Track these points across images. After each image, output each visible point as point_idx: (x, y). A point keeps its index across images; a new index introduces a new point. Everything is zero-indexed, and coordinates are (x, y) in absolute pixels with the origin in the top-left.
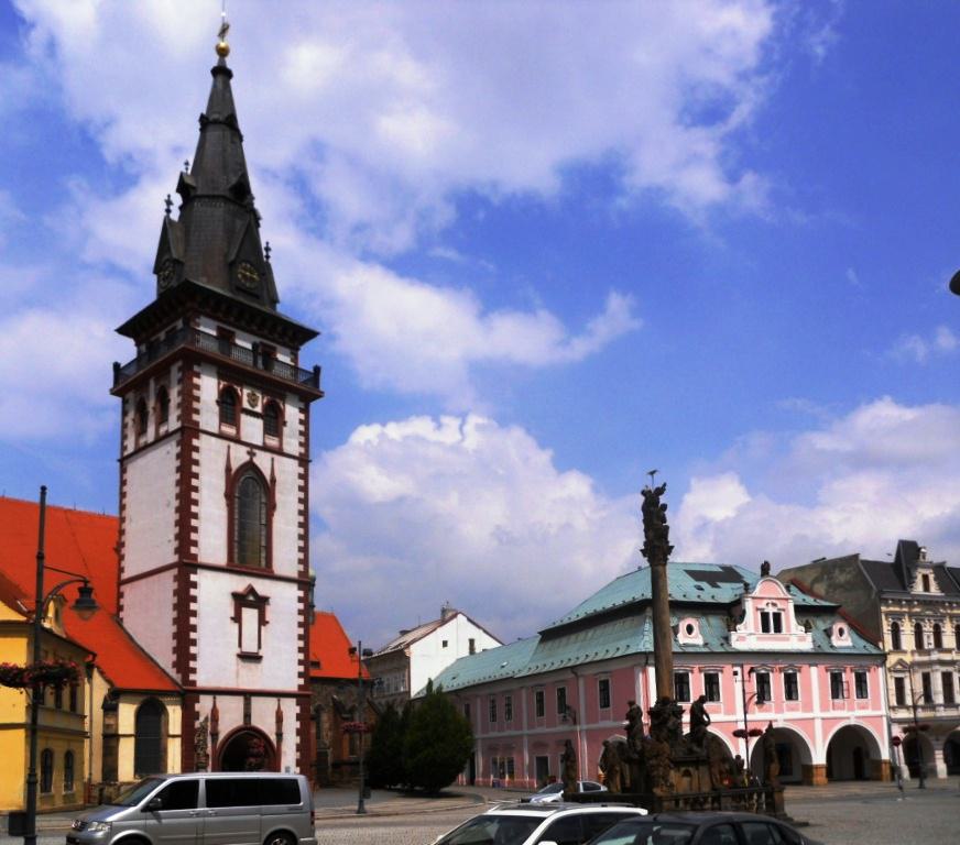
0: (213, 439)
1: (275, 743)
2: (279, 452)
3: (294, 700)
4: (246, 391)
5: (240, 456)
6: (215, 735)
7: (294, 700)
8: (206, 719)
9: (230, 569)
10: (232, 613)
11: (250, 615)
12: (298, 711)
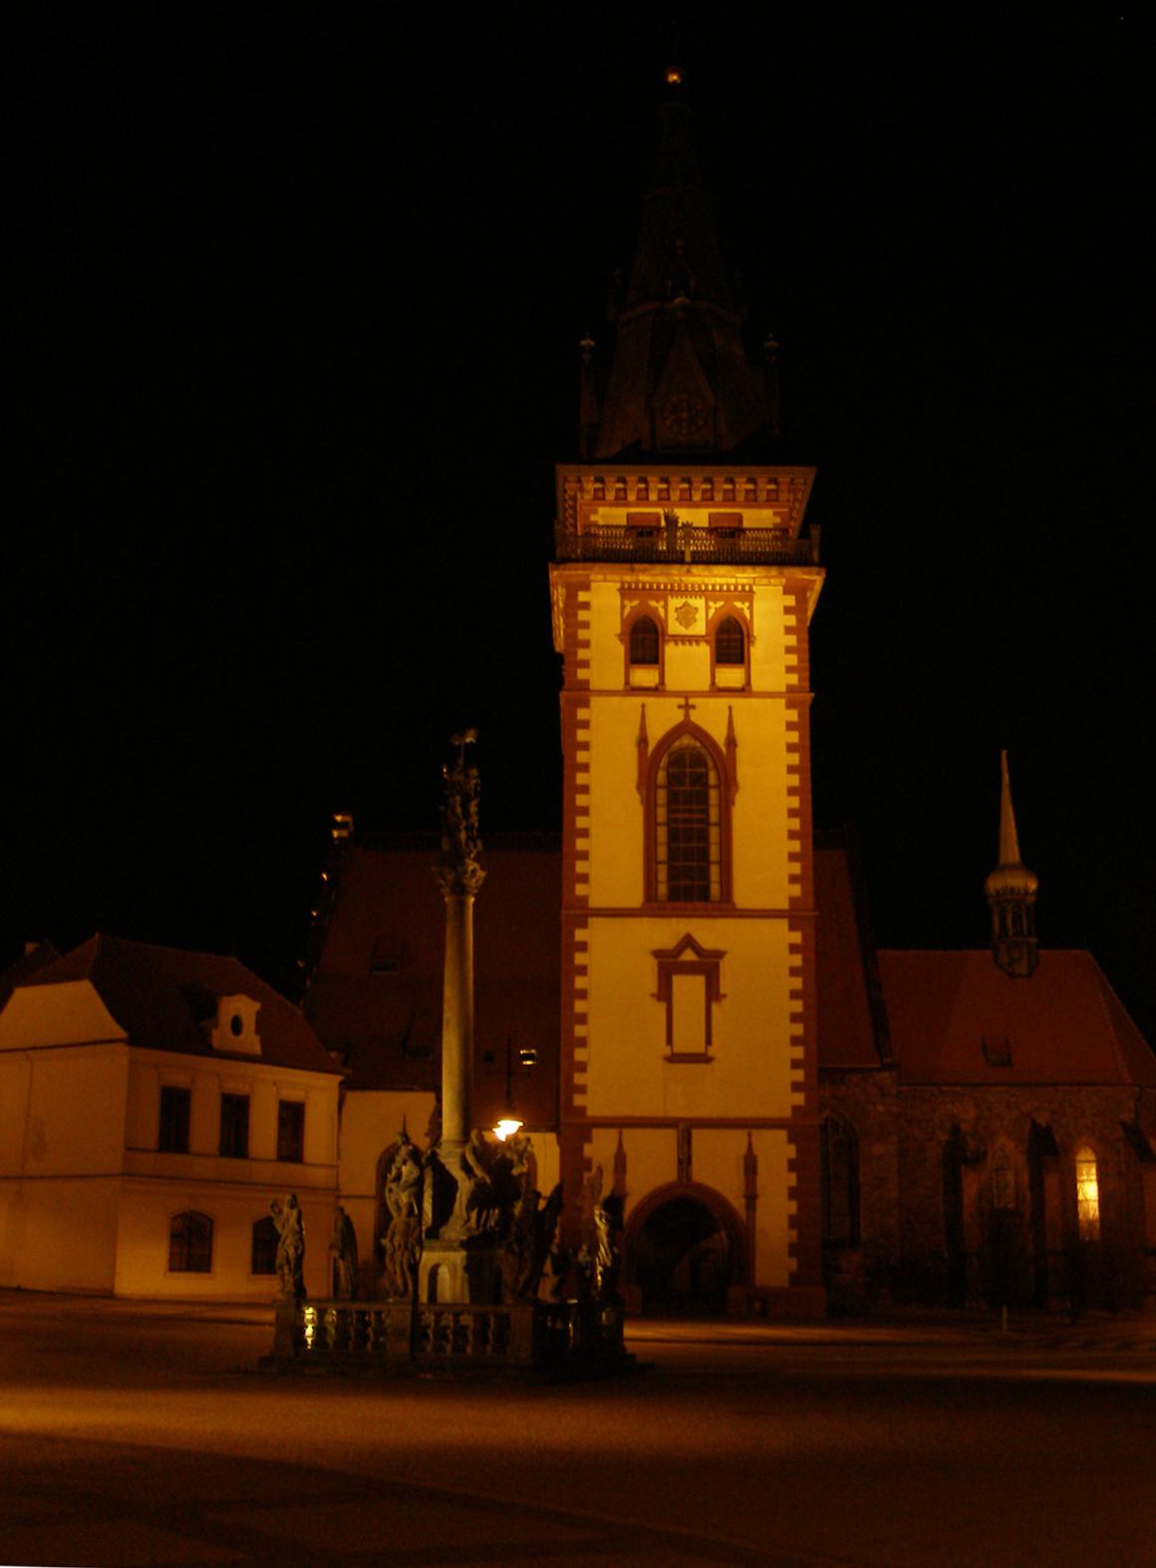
1: (743, 1213)
2: (744, 691)
3: (782, 1134)
5: (663, 716)
7: (782, 1134)
9: (652, 907)
10: (651, 984)
11: (689, 989)
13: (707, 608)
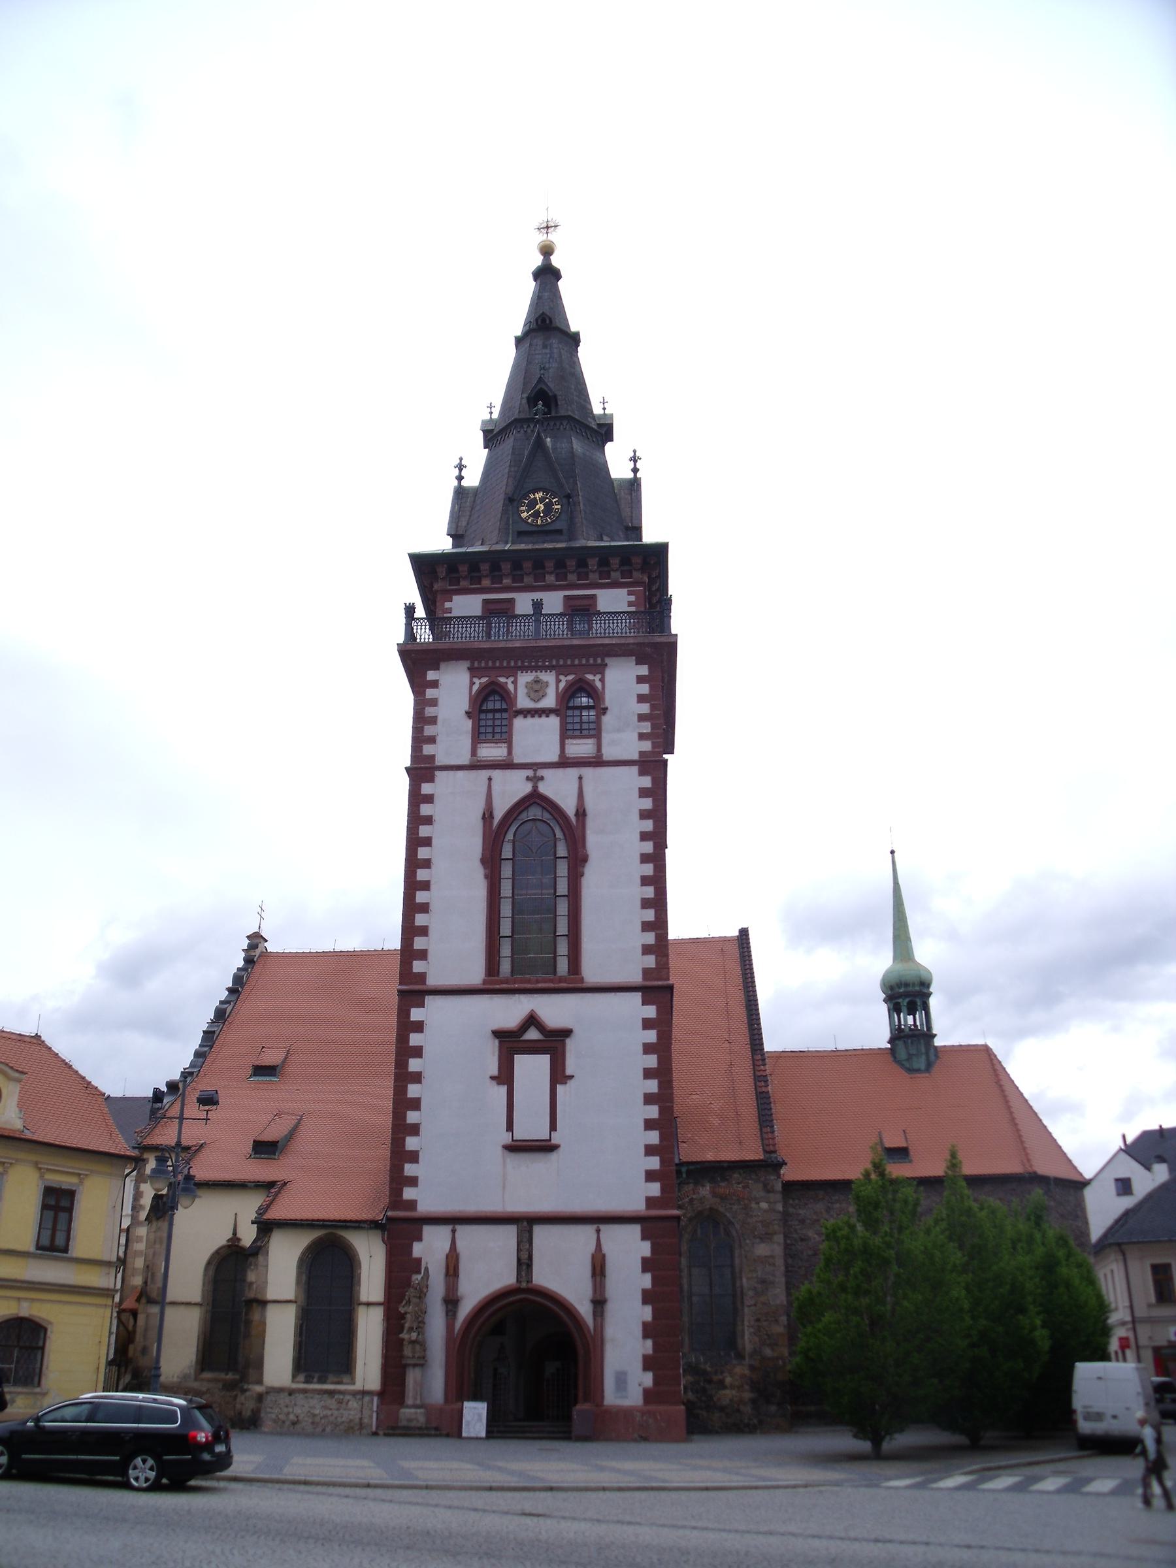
0: (460, 774)
2: (597, 761)
3: (636, 1229)
4: (525, 678)
5: (511, 788)
6: (451, 1302)
7: (636, 1229)
10: (493, 1066)
11: (532, 1069)
13: (558, 681)
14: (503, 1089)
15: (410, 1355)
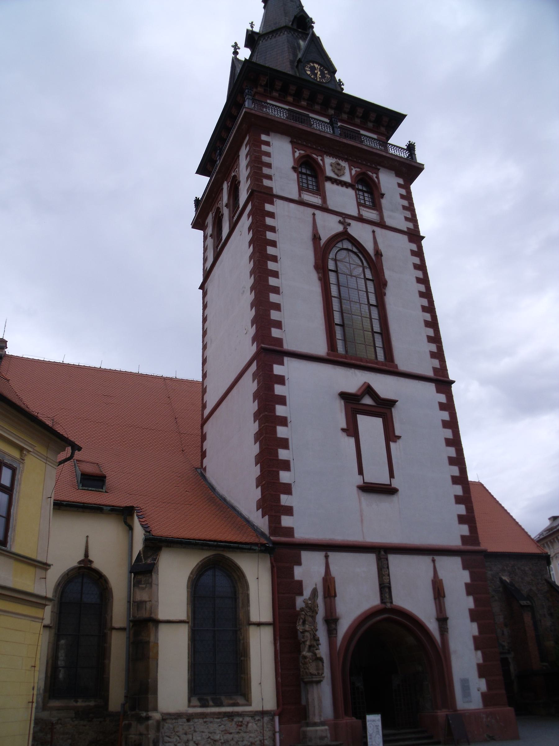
0: (292, 205)
6: (332, 621)
8: (314, 592)
9: (332, 359)
11: (370, 426)
12: (468, 580)
14: (352, 440)
15: (315, 672)
